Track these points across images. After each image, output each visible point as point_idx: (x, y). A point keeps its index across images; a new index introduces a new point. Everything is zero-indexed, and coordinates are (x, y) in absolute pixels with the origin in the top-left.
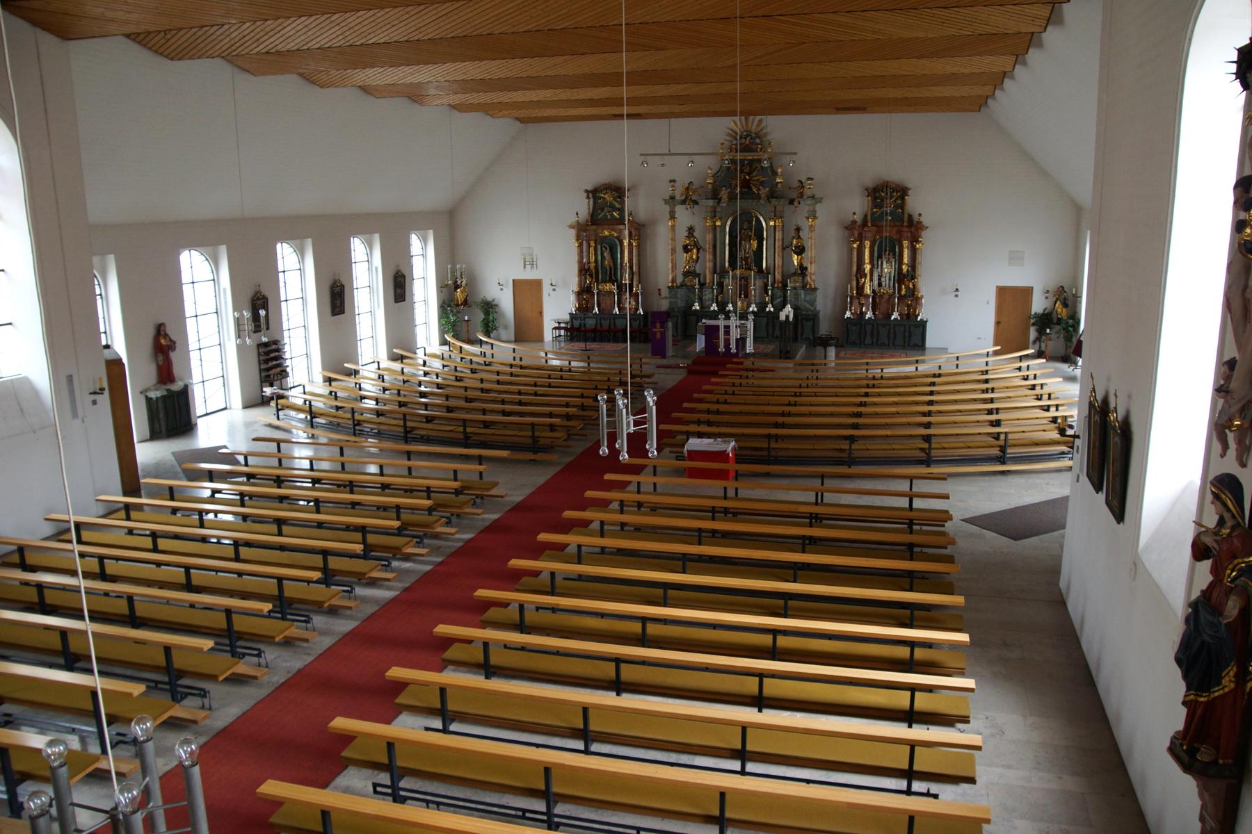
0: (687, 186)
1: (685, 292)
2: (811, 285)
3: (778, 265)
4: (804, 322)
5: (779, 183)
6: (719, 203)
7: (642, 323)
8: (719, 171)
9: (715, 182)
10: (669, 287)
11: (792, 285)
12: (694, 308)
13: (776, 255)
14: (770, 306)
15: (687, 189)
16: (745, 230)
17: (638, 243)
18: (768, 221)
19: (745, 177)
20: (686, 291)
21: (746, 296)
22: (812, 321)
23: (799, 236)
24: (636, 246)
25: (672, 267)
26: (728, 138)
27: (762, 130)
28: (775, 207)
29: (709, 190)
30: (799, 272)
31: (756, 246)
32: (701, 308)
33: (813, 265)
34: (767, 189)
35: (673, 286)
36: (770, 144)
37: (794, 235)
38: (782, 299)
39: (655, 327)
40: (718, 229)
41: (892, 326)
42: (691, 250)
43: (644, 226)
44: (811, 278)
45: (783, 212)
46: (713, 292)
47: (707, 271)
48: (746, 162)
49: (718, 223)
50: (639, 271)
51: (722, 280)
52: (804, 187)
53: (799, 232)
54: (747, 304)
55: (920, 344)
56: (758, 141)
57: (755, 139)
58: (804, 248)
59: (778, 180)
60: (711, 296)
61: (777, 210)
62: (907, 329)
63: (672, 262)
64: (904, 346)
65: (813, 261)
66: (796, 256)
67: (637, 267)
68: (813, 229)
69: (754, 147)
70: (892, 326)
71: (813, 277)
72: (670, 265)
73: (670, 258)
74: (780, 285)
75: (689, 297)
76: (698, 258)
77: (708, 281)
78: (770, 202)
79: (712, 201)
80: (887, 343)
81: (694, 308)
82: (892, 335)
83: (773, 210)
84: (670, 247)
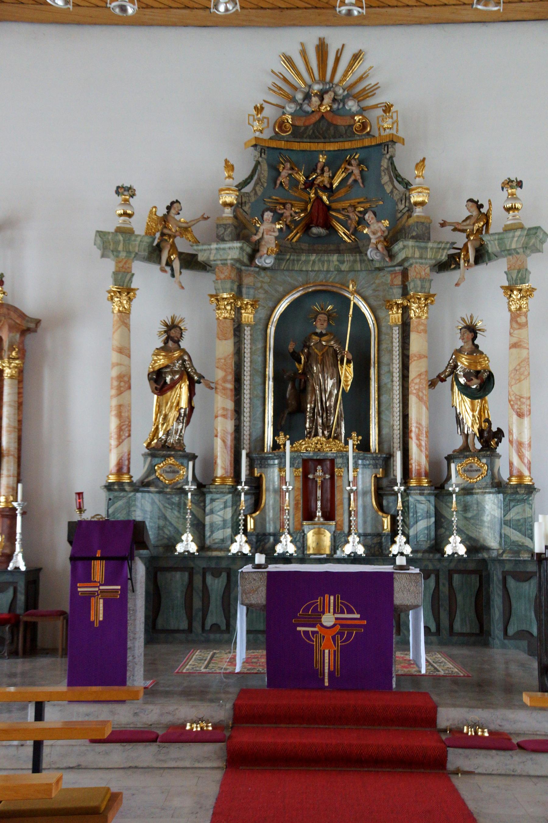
0: (162, 211)
1: (153, 503)
2: (521, 476)
3: (419, 424)
4: (512, 583)
5: (416, 204)
6: (252, 257)
7: (21, 598)
8: (251, 177)
9: (241, 204)
10: (109, 487)
11: (460, 480)
12: (180, 548)
13: (413, 400)
14: (400, 539)
15: (165, 219)
16: (321, 335)
17: (21, 371)
18: (382, 314)
19: (319, 199)
20: (157, 498)
21: (329, 515)
23: (477, 346)
24: (11, 377)
25: (120, 429)
26: (274, 99)
27: (361, 79)
28: (405, 274)
29: (230, 222)
30: (478, 446)
31: (350, 378)
32: (202, 547)
33: (526, 420)
34: (386, 223)
35: (120, 484)
36: (387, 108)
37: (460, 344)
38: (433, 520)
39: (88, 578)
40: (247, 332)
42: (174, 384)
43: (38, 322)
44: (521, 457)
45: (431, 281)
46: (236, 502)
47: (219, 442)
48: (322, 159)
49: (247, 316)
50: (19, 449)
51: (257, 473)
52: (487, 216)
53: (475, 337)
54: (334, 539)
56: (352, 105)
57: (343, 101)
58: (491, 376)
59: (415, 198)
60: (229, 513)
61: (412, 274)
63: (119, 415)
65: (525, 408)
66: (467, 400)
67: (15, 435)
68: (522, 320)
69: (340, 121)
71: (527, 454)
72: (114, 423)
73: (114, 402)
74: (425, 482)
75: (165, 518)
76: (191, 408)
77: (219, 472)
78: (392, 256)
79: (237, 244)
81: (180, 548)
83: (398, 280)
84: (114, 373)
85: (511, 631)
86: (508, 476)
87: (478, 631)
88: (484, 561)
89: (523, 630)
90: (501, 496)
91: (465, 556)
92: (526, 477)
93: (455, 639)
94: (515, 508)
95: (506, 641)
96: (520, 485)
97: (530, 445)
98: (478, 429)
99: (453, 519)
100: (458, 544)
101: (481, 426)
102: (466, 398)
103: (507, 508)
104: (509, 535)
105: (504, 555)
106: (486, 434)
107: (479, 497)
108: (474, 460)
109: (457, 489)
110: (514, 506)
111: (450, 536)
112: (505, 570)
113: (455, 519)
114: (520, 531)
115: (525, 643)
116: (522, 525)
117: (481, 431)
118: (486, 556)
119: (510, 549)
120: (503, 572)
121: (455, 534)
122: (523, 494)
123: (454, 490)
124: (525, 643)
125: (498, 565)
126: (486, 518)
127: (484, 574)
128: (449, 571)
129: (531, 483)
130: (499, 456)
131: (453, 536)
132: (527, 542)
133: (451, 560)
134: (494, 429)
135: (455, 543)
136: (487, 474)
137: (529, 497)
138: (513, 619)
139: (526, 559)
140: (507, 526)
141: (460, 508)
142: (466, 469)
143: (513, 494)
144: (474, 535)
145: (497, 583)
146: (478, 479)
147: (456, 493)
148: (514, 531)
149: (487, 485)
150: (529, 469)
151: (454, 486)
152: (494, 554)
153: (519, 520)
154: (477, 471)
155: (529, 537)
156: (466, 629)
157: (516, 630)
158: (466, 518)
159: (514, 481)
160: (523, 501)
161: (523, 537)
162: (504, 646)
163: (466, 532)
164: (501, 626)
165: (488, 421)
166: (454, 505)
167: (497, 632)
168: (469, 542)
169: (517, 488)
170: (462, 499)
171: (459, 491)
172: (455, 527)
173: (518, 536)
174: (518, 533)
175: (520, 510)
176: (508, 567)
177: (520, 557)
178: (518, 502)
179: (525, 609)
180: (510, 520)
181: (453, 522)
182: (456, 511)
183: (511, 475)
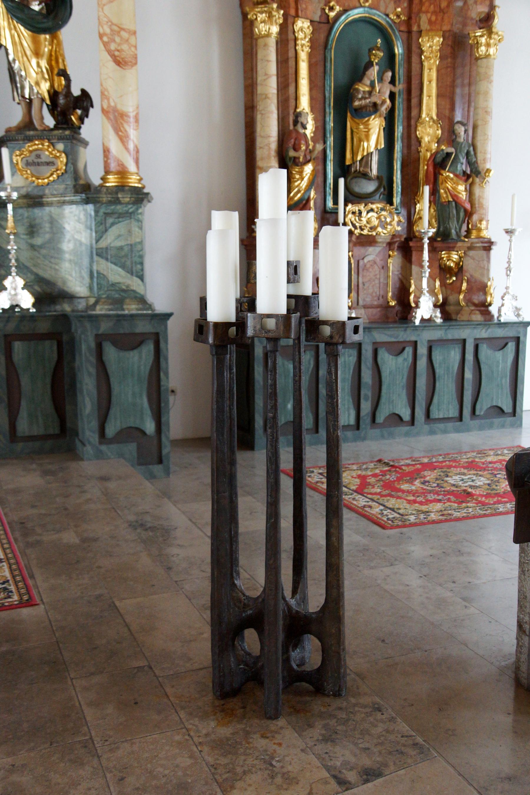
2: (123, 173)
11: (20, 181)
22: (148, 348)
30: (50, 121)
41: (422, 350)
44: (123, 139)
55: (507, 408)
62: (470, 357)
64: (460, 418)
70: (422, 350)
71: (132, 133)
80: (406, 414)
82: (422, 383)
85: (111, 430)
86: (102, 173)
87: (57, 431)
88: (64, 317)
89: (131, 427)
90: (90, 208)
91: (33, 310)
92: (132, 174)
93: (20, 446)
94: (114, 228)
95: (104, 448)
96: (121, 187)
97: (137, 121)
98: (49, 92)
99: (9, 247)
100: (19, 290)
101: (52, 86)
102: (22, 28)
103: (102, 228)
104: (105, 273)
105: (98, 307)
106: (61, 101)
107: (53, 210)
108: (43, 145)
109: (15, 195)
110: (113, 224)
111: (5, 277)
112: (100, 332)
113: (12, 247)
114: (123, 267)
115: (131, 448)
116: (126, 256)
117: (54, 95)
118: (67, 308)
119: (108, 297)
120: (97, 336)
121: (14, 274)
122: (128, 203)
123: (9, 196)
124: (131, 448)
125: (88, 325)
126: (67, 246)
127: (65, 338)
128: (6, 336)
129: (140, 186)
130: (85, 144)
131: (10, 278)
132: (135, 284)
133: (9, 317)
134: (76, 92)
135: (15, 289)
136: (66, 170)
137: (137, 209)
138: (114, 411)
139: (134, 312)
140: (102, 257)
141: (21, 230)
142: (30, 160)
143: (110, 203)
144: (46, 274)
145: (88, 354)
146: (51, 179)
147: (13, 202)
148: (113, 266)
149: (66, 188)
150: (137, 161)
151: (9, 190)
152: (81, 305)
153: (121, 248)
154: (48, 164)
155: (138, 276)
156: (38, 430)
157: (118, 428)
158: (33, 247)
159: (112, 181)
160: (129, 215)
161: (129, 275)
162: (99, 455)
163: (35, 270)
164: (94, 424)
165: (63, 73)
166: (10, 223)
167: (88, 433)
168: (40, 287)
169: (117, 193)
170: (25, 213)
171: (19, 198)
172: (13, 261)
173: (119, 275)
174: (120, 270)
175: (123, 231)
176: (105, 327)
177: (123, 310)
178: (119, 218)
179: (134, 394)
180: (107, 248)
181: (9, 252)
182: (15, 234)
183: (107, 172)
